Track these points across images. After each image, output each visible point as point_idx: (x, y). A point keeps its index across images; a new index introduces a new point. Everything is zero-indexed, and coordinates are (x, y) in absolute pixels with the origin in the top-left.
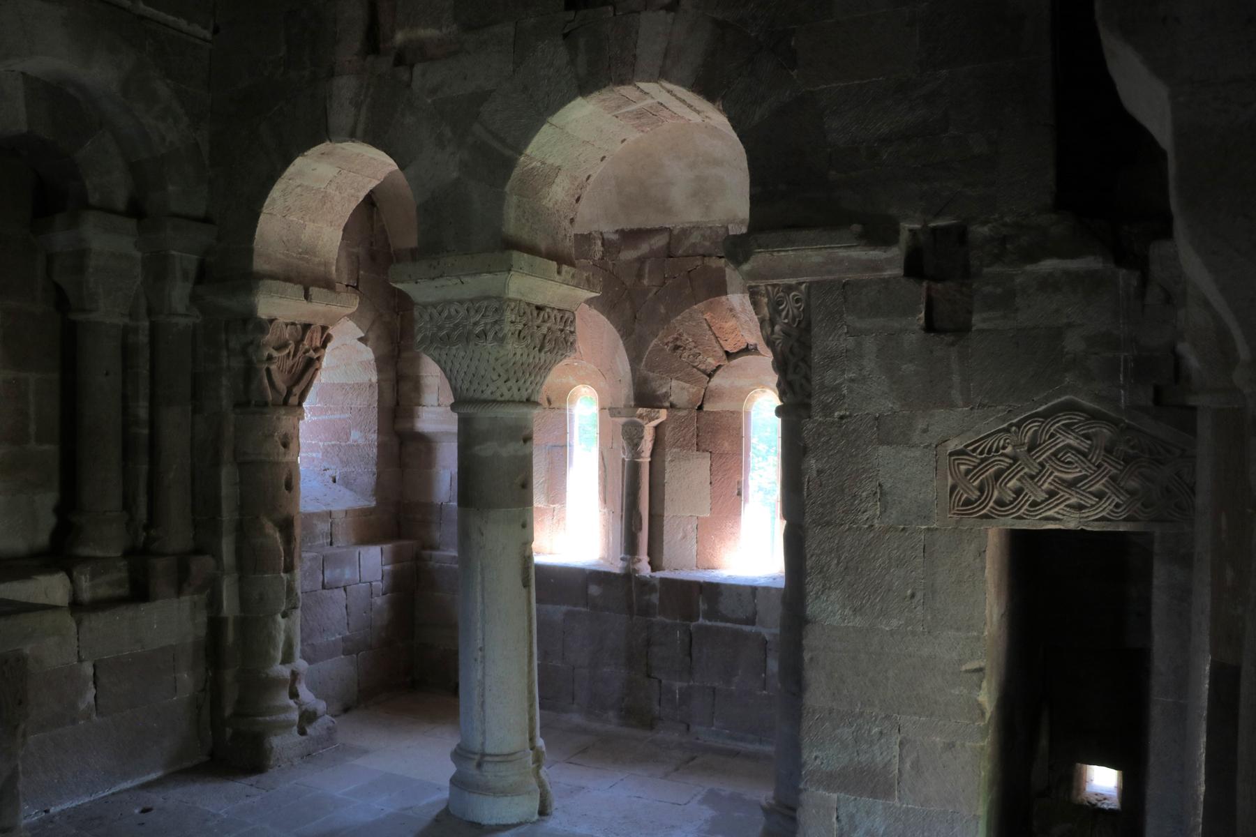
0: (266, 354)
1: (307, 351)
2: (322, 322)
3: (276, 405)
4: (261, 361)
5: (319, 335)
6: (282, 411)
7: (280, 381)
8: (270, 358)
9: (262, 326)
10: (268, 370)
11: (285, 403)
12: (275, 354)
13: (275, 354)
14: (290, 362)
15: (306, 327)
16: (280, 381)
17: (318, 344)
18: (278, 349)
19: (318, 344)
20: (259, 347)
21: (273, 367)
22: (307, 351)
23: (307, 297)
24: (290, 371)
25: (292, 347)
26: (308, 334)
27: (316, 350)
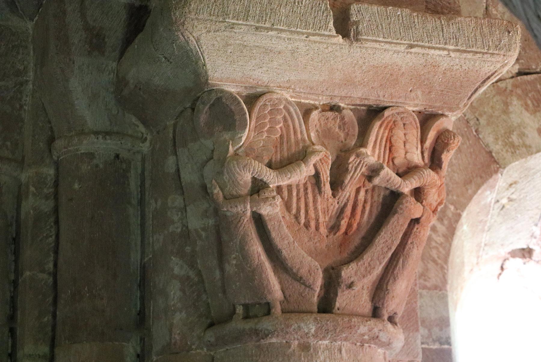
0: (246, 178)
1: (373, 172)
2: (414, 105)
3: (293, 310)
4: (233, 198)
5: (414, 134)
6: (310, 326)
7: (305, 253)
8: (258, 187)
9: (226, 113)
10: (259, 221)
11: (326, 306)
12: (273, 179)
13: (273, 179)
14: (327, 204)
15: (372, 113)
16: (305, 253)
17: (416, 157)
18: (280, 165)
19: (416, 157)
20: (220, 161)
21: (272, 210)
22: (373, 172)
23: (344, 26)
24: (334, 228)
25: (322, 159)
26: (377, 131)
27: (407, 171)
